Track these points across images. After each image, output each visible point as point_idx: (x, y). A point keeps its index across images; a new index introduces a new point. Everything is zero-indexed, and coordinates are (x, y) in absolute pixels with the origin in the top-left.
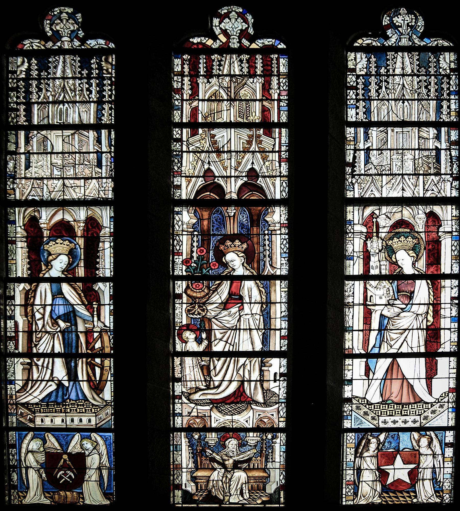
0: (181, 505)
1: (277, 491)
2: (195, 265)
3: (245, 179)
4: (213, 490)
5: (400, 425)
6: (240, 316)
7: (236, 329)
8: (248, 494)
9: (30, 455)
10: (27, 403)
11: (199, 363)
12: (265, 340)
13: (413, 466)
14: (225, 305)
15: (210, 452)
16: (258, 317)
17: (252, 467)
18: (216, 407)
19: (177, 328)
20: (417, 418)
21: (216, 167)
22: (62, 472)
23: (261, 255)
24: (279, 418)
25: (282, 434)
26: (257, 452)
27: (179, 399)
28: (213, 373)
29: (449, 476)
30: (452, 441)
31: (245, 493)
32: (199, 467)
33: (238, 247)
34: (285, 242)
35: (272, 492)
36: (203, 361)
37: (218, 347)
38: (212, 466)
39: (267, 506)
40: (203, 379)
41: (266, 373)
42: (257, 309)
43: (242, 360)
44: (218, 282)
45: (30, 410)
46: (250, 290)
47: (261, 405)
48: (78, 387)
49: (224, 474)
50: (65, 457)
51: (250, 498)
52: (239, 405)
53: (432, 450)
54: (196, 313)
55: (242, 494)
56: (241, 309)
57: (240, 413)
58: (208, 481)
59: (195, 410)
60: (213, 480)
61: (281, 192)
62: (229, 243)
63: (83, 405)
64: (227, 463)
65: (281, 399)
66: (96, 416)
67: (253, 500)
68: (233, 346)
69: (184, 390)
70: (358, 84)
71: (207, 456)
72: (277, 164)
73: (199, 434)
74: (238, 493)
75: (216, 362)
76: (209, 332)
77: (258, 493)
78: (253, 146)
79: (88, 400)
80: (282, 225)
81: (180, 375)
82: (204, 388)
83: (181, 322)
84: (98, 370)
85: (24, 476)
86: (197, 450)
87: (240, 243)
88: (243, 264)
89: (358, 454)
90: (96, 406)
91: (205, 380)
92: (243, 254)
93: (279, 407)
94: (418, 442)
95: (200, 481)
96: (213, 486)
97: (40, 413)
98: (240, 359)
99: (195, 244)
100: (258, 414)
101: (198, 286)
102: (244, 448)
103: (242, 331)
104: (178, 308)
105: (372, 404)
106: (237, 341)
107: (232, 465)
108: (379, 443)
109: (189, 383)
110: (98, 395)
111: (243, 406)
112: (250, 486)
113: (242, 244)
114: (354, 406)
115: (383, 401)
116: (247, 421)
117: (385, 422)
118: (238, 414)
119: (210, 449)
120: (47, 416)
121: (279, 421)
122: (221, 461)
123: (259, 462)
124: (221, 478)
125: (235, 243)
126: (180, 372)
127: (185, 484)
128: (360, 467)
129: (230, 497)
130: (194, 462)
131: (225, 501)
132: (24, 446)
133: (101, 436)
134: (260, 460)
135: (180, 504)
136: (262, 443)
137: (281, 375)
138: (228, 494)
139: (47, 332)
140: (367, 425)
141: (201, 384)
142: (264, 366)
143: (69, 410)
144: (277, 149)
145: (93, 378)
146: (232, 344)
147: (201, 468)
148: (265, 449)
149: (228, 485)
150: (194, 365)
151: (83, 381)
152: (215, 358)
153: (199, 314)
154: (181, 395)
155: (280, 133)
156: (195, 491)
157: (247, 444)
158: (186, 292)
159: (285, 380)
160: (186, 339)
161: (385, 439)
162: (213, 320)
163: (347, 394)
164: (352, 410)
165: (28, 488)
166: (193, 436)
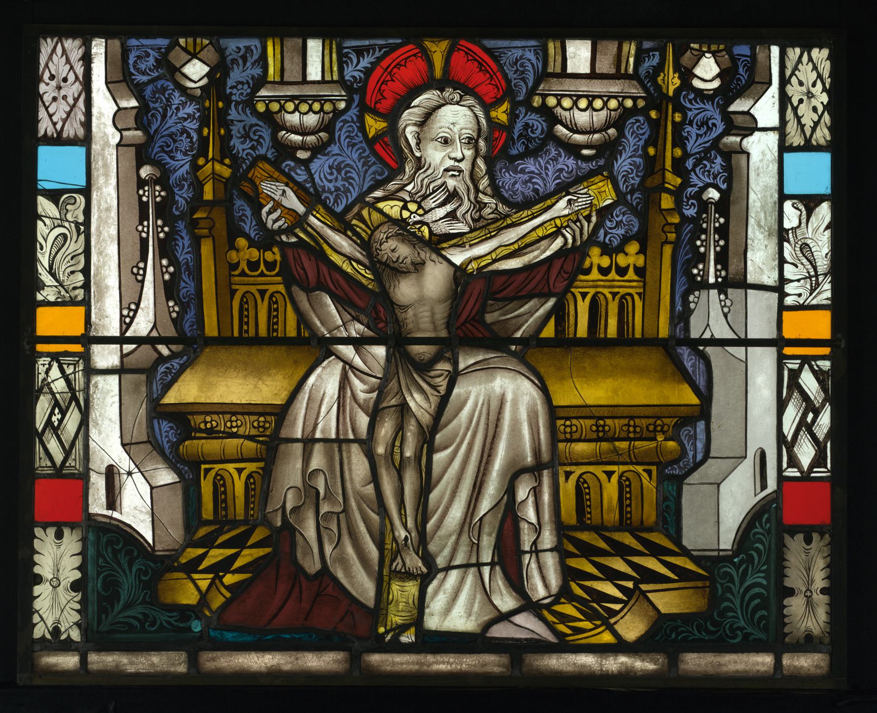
0: (69, 661)
4: (310, 531)
8: (550, 561)
15: (293, 202)
17: (582, 331)
25: (794, 53)
26: (621, 199)
31: (536, 551)
32: (211, 329)
35: (727, 542)
38: (302, 320)
49: (381, 390)
51: (564, 593)
60: (309, 442)
73: (210, 53)
74: (487, 556)
77: (623, 551)
86: (198, 186)
95: (211, 446)
102: (530, 165)
107: (441, 311)
112: (568, 488)
119: (291, 181)
122: (365, 275)
123: (630, 284)
124: (363, 421)
127: (111, 473)
129: (425, 581)
131: (396, 618)
134: (640, 272)
135: (67, 646)
136: (656, 126)
138: (414, 562)
147: (224, 341)
148: (673, 181)
156: (176, 533)
157: (551, 136)
166: (174, 71)
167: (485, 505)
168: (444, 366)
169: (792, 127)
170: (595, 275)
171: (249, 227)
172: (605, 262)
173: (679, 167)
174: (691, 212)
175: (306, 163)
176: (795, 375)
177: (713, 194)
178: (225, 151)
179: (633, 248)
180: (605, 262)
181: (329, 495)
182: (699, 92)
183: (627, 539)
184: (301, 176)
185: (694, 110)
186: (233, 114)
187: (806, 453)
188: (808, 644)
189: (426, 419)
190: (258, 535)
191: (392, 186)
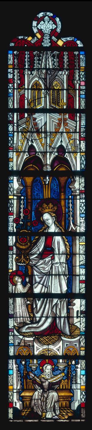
0: (12, 421)
1: (79, 407)
2: (22, 223)
4: (35, 408)
6: (52, 264)
7: (49, 274)
8: (58, 411)
11: (25, 302)
12: (70, 284)
14: (42, 256)
16: (64, 265)
17: (61, 388)
18: (38, 339)
19: (10, 274)
24: (80, 347)
25: (82, 361)
26: (65, 375)
27: (12, 332)
31: (57, 410)
32: (25, 388)
33: (51, 208)
35: (76, 409)
36: (28, 301)
37: (37, 290)
38: (34, 387)
39: (72, 420)
40: (28, 316)
41: (71, 311)
42: (63, 259)
43: (55, 301)
44: (37, 237)
46: (58, 243)
47: (68, 337)
49: (42, 394)
51: (60, 414)
52: (53, 337)
54: (22, 262)
55: (54, 411)
56: (53, 258)
57: (54, 343)
58: (31, 400)
59: (23, 341)
60: (35, 399)
64: (44, 384)
65: (81, 332)
67: (62, 416)
68: (47, 288)
69: (16, 324)
71: (30, 379)
74: (52, 410)
75: (37, 301)
76: (32, 276)
77: (66, 410)
81: (12, 312)
82: (29, 322)
83: (12, 269)
86: (24, 374)
87: (52, 206)
88: (54, 222)
91: (30, 317)
92: (54, 215)
93: (80, 338)
96: (35, 404)
98: (54, 299)
99: (22, 206)
101: (23, 240)
102: (56, 372)
103: (53, 276)
104: (10, 258)
106: (50, 284)
107: (48, 386)
109: (18, 319)
111: (56, 337)
112: (60, 404)
113: (54, 206)
116: (58, 350)
118: (52, 344)
119: (33, 373)
121: (80, 350)
123: (66, 383)
124: (40, 397)
125: (49, 206)
126: (12, 310)
127: (15, 402)
129: (46, 413)
130: (21, 384)
131: (43, 416)
135: (11, 419)
137: (82, 312)
138: (45, 411)
141: (27, 320)
142: (70, 306)
146: (47, 287)
148: (70, 373)
149: (45, 403)
150: (22, 304)
152: (36, 299)
153: (24, 262)
154: (13, 329)
156: (22, 408)
157: (58, 368)
158: (15, 245)
159: (84, 317)
160: (15, 283)
162: (34, 267)
167: (52, 405)
168: (48, 392)
169: (82, 368)
170: (63, 382)
171: (29, 378)
172: (64, 381)
173: (71, 372)
174: (72, 376)
175: (34, 372)
176: (82, 392)
177: (74, 375)
178: (26, 370)
179: (66, 380)
180: (64, 381)
181: (37, 405)
182: (73, 364)
183: (66, 409)
184: (34, 373)
185: (72, 366)
186: (27, 367)
187: (83, 400)
188: (83, 419)
189: (46, 397)
190: (30, 408)
191: (43, 374)
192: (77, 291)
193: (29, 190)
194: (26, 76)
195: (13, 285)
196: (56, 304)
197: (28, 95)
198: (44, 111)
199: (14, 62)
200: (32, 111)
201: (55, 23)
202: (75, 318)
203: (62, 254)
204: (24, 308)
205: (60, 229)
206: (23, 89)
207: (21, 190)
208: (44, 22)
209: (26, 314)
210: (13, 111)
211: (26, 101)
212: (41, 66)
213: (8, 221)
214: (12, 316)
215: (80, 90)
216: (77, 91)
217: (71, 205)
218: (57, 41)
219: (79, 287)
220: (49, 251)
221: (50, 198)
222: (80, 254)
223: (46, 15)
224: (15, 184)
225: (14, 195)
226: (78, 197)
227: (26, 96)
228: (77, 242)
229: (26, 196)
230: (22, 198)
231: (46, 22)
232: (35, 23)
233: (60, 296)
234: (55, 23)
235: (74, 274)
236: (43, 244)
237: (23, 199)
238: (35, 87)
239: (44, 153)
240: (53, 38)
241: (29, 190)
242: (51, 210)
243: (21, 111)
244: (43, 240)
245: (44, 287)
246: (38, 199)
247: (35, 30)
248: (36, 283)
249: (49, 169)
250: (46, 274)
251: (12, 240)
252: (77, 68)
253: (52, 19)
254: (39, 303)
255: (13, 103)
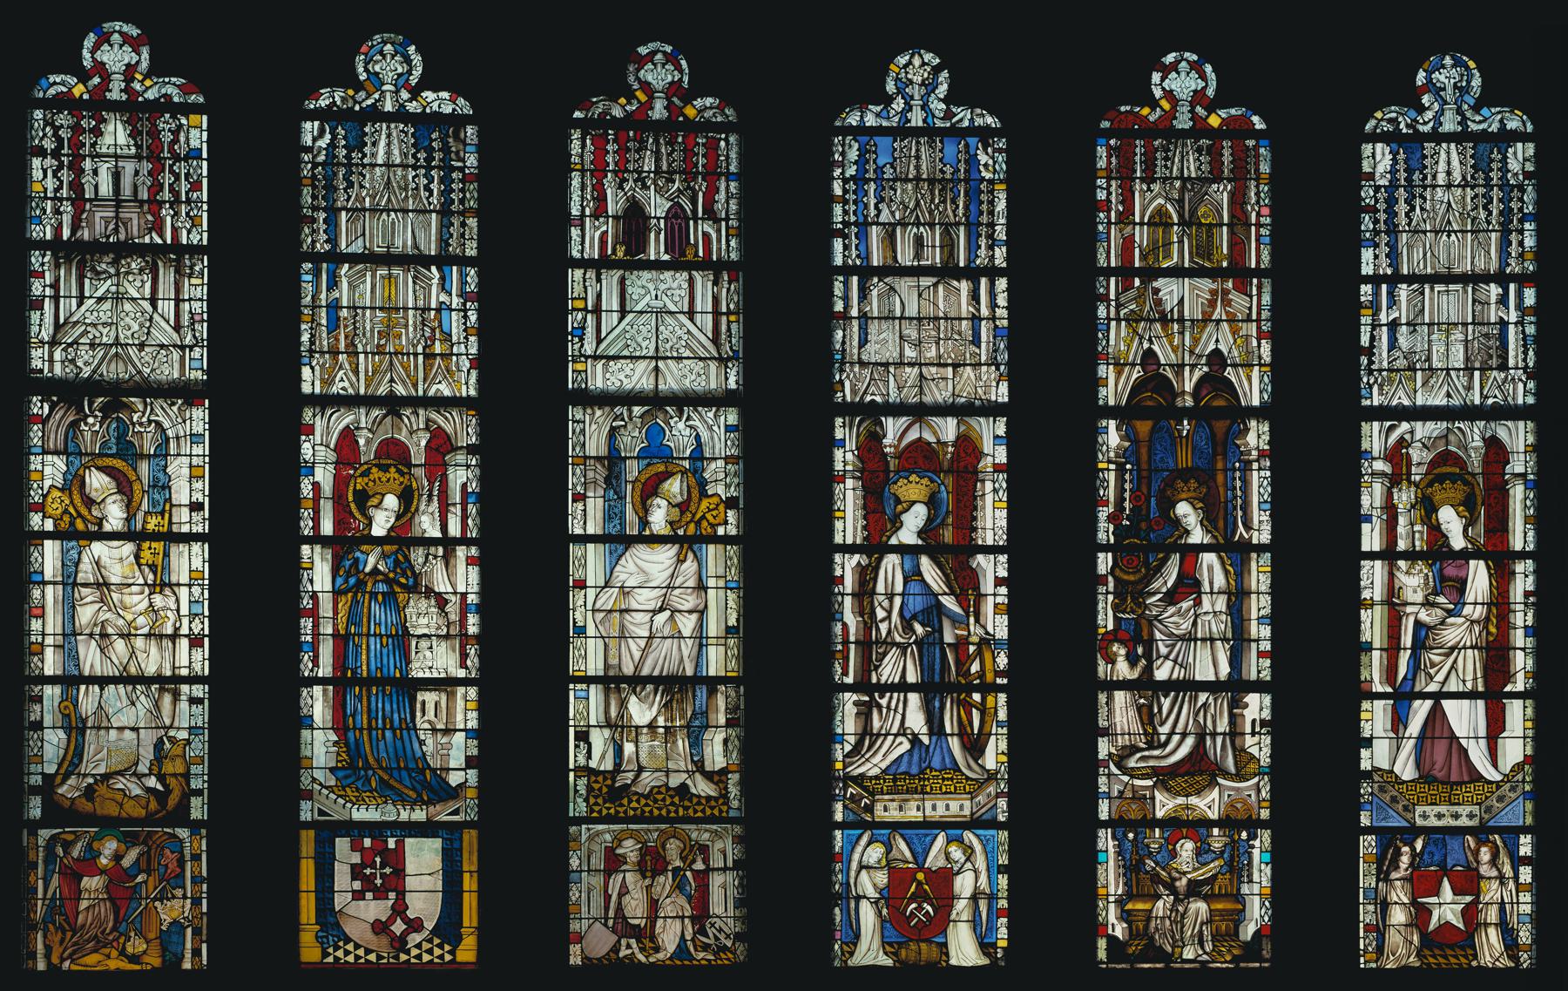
3: (1205, 369)
5: (1448, 822)
6: (1197, 616)
7: (1189, 638)
9: (864, 872)
10: (862, 776)
12: (1236, 660)
13: (1469, 899)
14: (1172, 598)
16: (1224, 617)
20: (1476, 809)
21: (1162, 346)
22: (914, 905)
23: (1230, 505)
28: (1157, 720)
29: (1527, 919)
30: (1529, 854)
34: (1265, 482)
36: (1140, 697)
37: (1161, 674)
41: (1239, 720)
42: (1221, 603)
43: (1203, 697)
44: (1161, 555)
45: (865, 789)
46: (1210, 568)
48: (944, 745)
50: (920, 876)
53: (1498, 869)
56: (1198, 603)
61: (1261, 392)
62: (1180, 484)
63: (952, 779)
66: (972, 799)
69: (1113, 750)
70: (1377, 201)
72: (1255, 343)
76: (1150, 643)
78: (1218, 310)
79: (960, 771)
80: (1262, 454)
81: (1106, 723)
84: (976, 714)
85: (853, 913)
88: (1201, 522)
89: (1383, 876)
90: (972, 780)
91: (1146, 733)
92: (1201, 505)
94: (1476, 853)
97: (882, 794)
100: (1226, 793)
105: (1404, 782)
108: (1414, 854)
110: (976, 761)
114: (1376, 786)
115: (1420, 777)
117: (1425, 816)
120: (893, 800)
128: (1385, 899)
132: (856, 857)
133: (978, 836)
137: (1263, 723)
139: (895, 644)
140: (1396, 822)
143: (928, 789)
144: (1254, 317)
145: (969, 729)
151: (952, 735)
153: (1133, 612)
155: (1259, 287)
158: (1112, 572)
159: (1268, 732)
161: (1424, 847)
163: (1365, 765)
164: (1372, 794)
165: (858, 936)
192: (1253, 676)
193: (1144, 451)
194: (1137, 194)
195: (1107, 663)
196: (1204, 705)
197: (1141, 236)
198: (1177, 272)
199: (1109, 163)
200: (1150, 273)
201: (1203, 76)
202: (1248, 737)
203: (1219, 593)
204: (1132, 713)
205: (1214, 537)
206: (1129, 224)
207: (1126, 450)
208: (1178, 73)
209: (1136, 727)
210: (1108, 272)
211: (1137, 250)
212: (1171, 172)
213: (1095, 520)
214: (1105, 732)
215: (1259, 225)
216: (1253, 228)
217: (1238, 484)
218: (1207, 117)
219: (1258, 667)
220: (1188, 586)
221: (1192, 468)
222: (1258, 593)
223: (1183, 59)
224: (1112, 437)
225: (1109, 462)
226: (1255, 465)
227: (1137, 239)
228: (1254, 565)
229: (1137, 463)
230: (1128, 466)
231: (1183, 75)
232: (1156, 77)
233: (1213, 687)
234: (1203, 76)
235: (1246, 636)
236: (1176, 569)
237: (1131, 470)
238: (1157, 220)
239: (1179, 368)
240: (1199, 109)
241: (1144, 451)
242: (1191, 494)
243: (1125, 272)
244: (1174, 561)
245: (1177, 667)
246: (1163, 470)
247: (1158, 93)
248: (1159, 657)
249: (1189, 402)
250: (1181, 638)
251: (1104, 562)
252: (1253, 176)
253: (1196, 67)
254: (1166, 703)
255: (1108, 255)
